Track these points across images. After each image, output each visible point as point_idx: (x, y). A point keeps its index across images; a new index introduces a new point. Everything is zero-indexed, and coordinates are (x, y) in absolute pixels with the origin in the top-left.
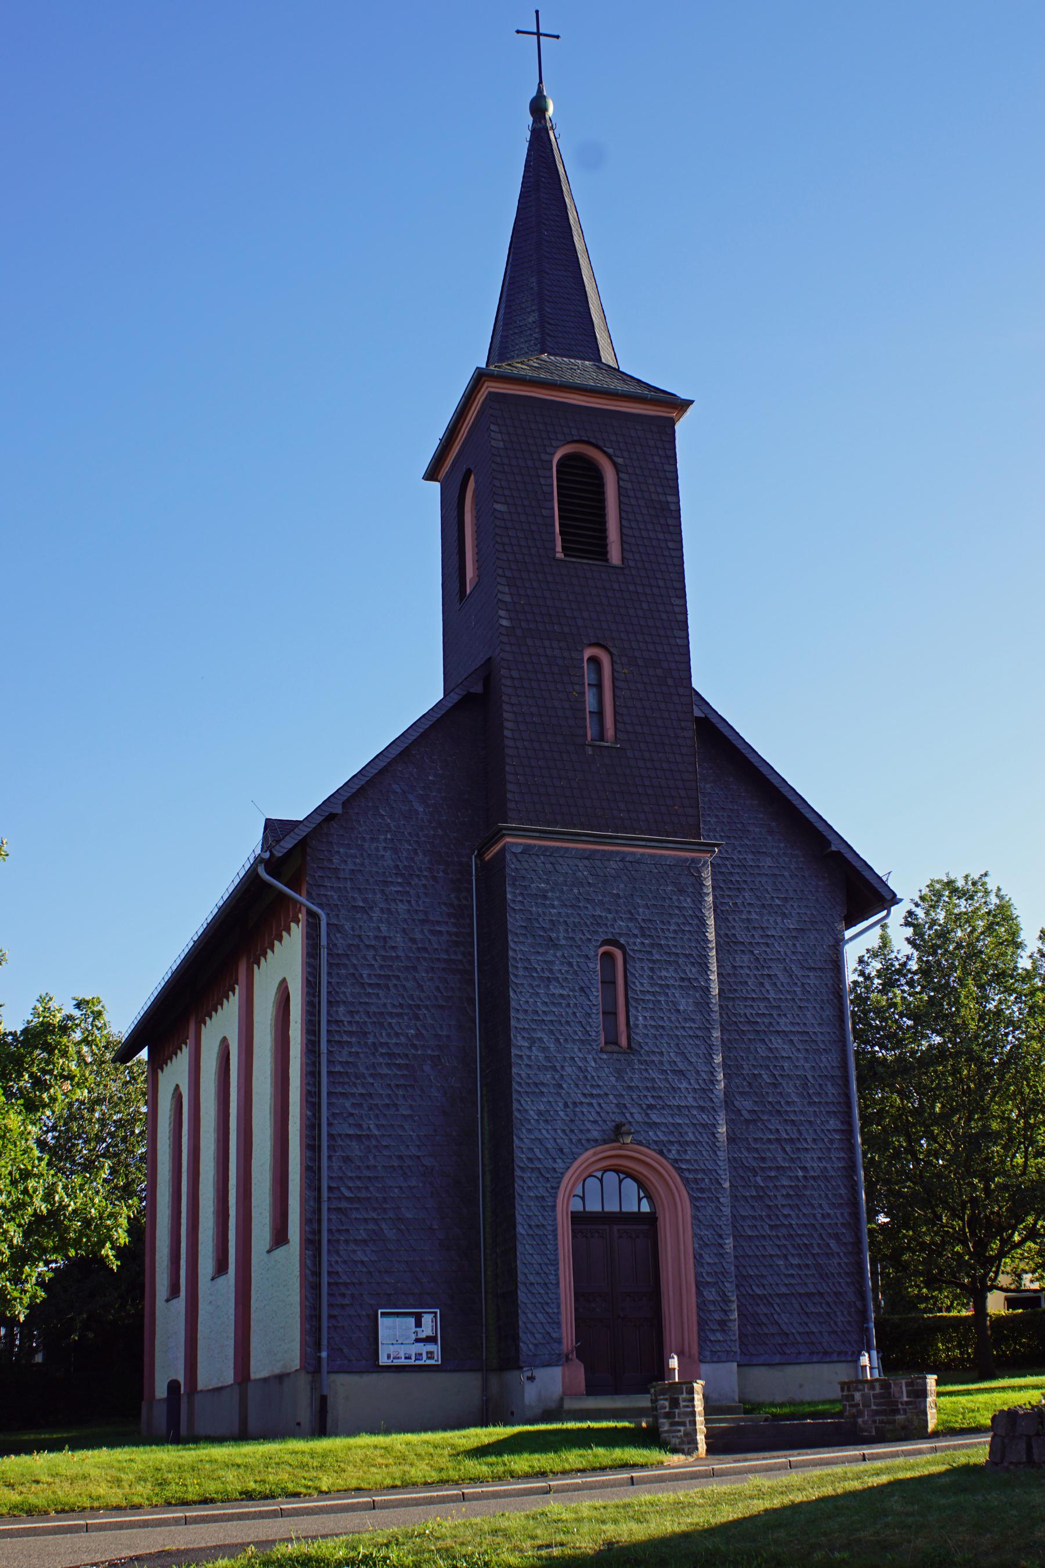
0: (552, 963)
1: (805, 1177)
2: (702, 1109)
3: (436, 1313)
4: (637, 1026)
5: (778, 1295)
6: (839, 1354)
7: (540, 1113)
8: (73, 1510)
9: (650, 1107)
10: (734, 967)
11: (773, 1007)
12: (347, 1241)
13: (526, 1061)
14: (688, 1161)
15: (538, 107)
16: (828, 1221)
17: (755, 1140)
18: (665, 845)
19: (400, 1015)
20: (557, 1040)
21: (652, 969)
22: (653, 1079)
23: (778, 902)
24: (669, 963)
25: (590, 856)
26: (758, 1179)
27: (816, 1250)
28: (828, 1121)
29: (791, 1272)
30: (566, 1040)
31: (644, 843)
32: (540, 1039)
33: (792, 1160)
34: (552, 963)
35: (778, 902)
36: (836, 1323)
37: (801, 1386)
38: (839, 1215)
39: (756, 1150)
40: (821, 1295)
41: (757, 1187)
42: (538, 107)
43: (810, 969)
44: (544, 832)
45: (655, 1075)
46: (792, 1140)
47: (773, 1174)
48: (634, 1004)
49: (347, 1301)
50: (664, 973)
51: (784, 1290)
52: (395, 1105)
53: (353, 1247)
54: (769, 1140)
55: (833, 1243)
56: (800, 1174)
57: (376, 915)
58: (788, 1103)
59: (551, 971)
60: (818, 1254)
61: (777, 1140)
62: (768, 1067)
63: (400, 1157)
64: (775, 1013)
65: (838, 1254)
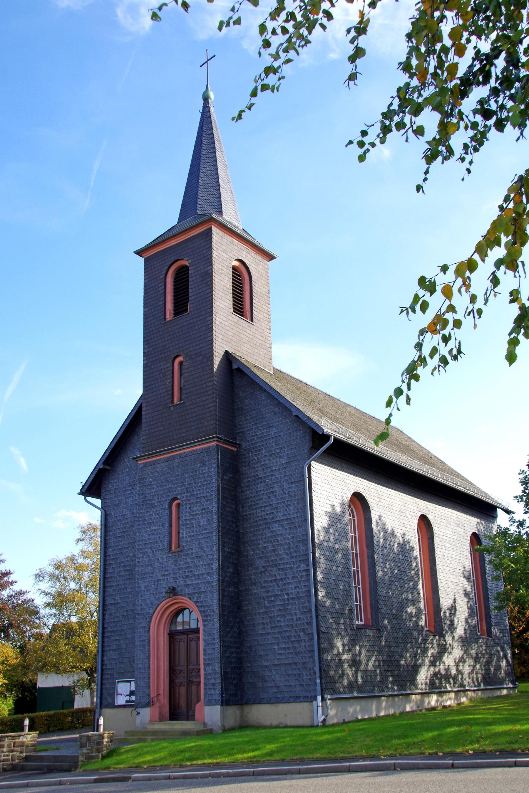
0: (152, 515)
1: (288, 599)
2: (208, 574)
3: (118, 682)
4: (183, 538)
5: (274, 665)
6: (304, 697)
7: (145, 587)
8: (337, 760)
9: (187, 577)
10: (257, 492)
11: (274, 509)
12: (109, 650)
13: (141, 564)
14: (201, 602)
15: (206, 99)
16: (299, 622)
17: (265, 581)
18: (184, 447)
19: (128, 548)
20: (153, 551)
21: (190, 508)
22: (188, 563)
23: (278, 451)
24: (197, 503)
25: (167, 460)
26: (266, 602)
27: (293, 639)
28: (300, 566)
29: (280, 652)
30: (156, 551)
31: (186, 447)
32: (147, 552)
33: (281, 590)
34: (152, 515)
35: (278, 451)
36: (303, 680)
37: (286, 715)
38: (304, 618)
39: (265, 587)
40: (295, 664)
41: (266, 607)
42: (206, 99)
43: (292, 483)
44: (171, 449)
45: (189, 560)
46: (282, 579)
47: (273, 599)
48: (182, 527)
49: (109, 677)
50: (195, 509)
51: (276, 662)
52: (126, 588)
53: (111, 652)
54: (271, 581)
55: (302, 634)
56: (286, 597)
57: (122, 506)
58: (280, 559)
59: (151, 519)
60: (294, 641)
61: (274, 580)
62: (271, 541)
63: (127, 611)
64: (275, 511)
65: (304, 640)
